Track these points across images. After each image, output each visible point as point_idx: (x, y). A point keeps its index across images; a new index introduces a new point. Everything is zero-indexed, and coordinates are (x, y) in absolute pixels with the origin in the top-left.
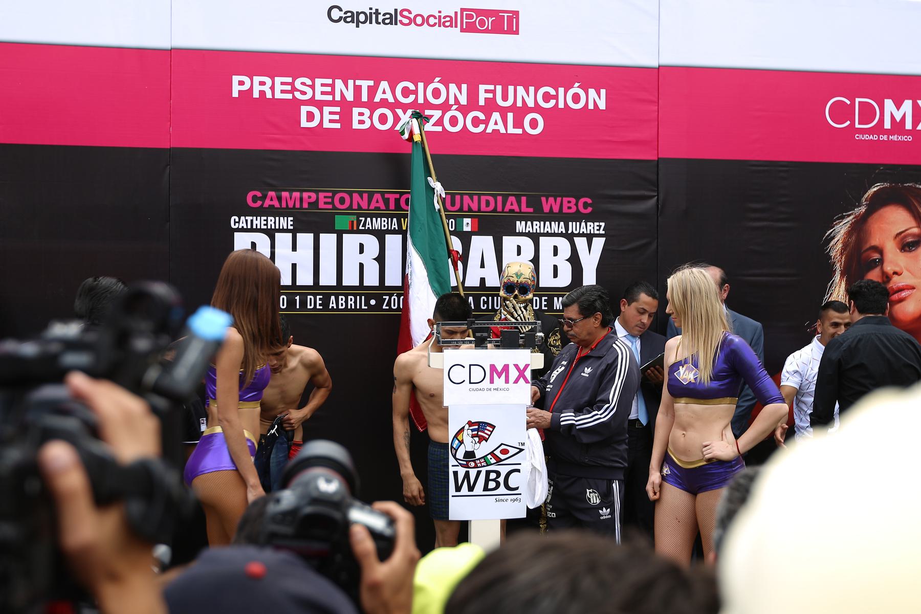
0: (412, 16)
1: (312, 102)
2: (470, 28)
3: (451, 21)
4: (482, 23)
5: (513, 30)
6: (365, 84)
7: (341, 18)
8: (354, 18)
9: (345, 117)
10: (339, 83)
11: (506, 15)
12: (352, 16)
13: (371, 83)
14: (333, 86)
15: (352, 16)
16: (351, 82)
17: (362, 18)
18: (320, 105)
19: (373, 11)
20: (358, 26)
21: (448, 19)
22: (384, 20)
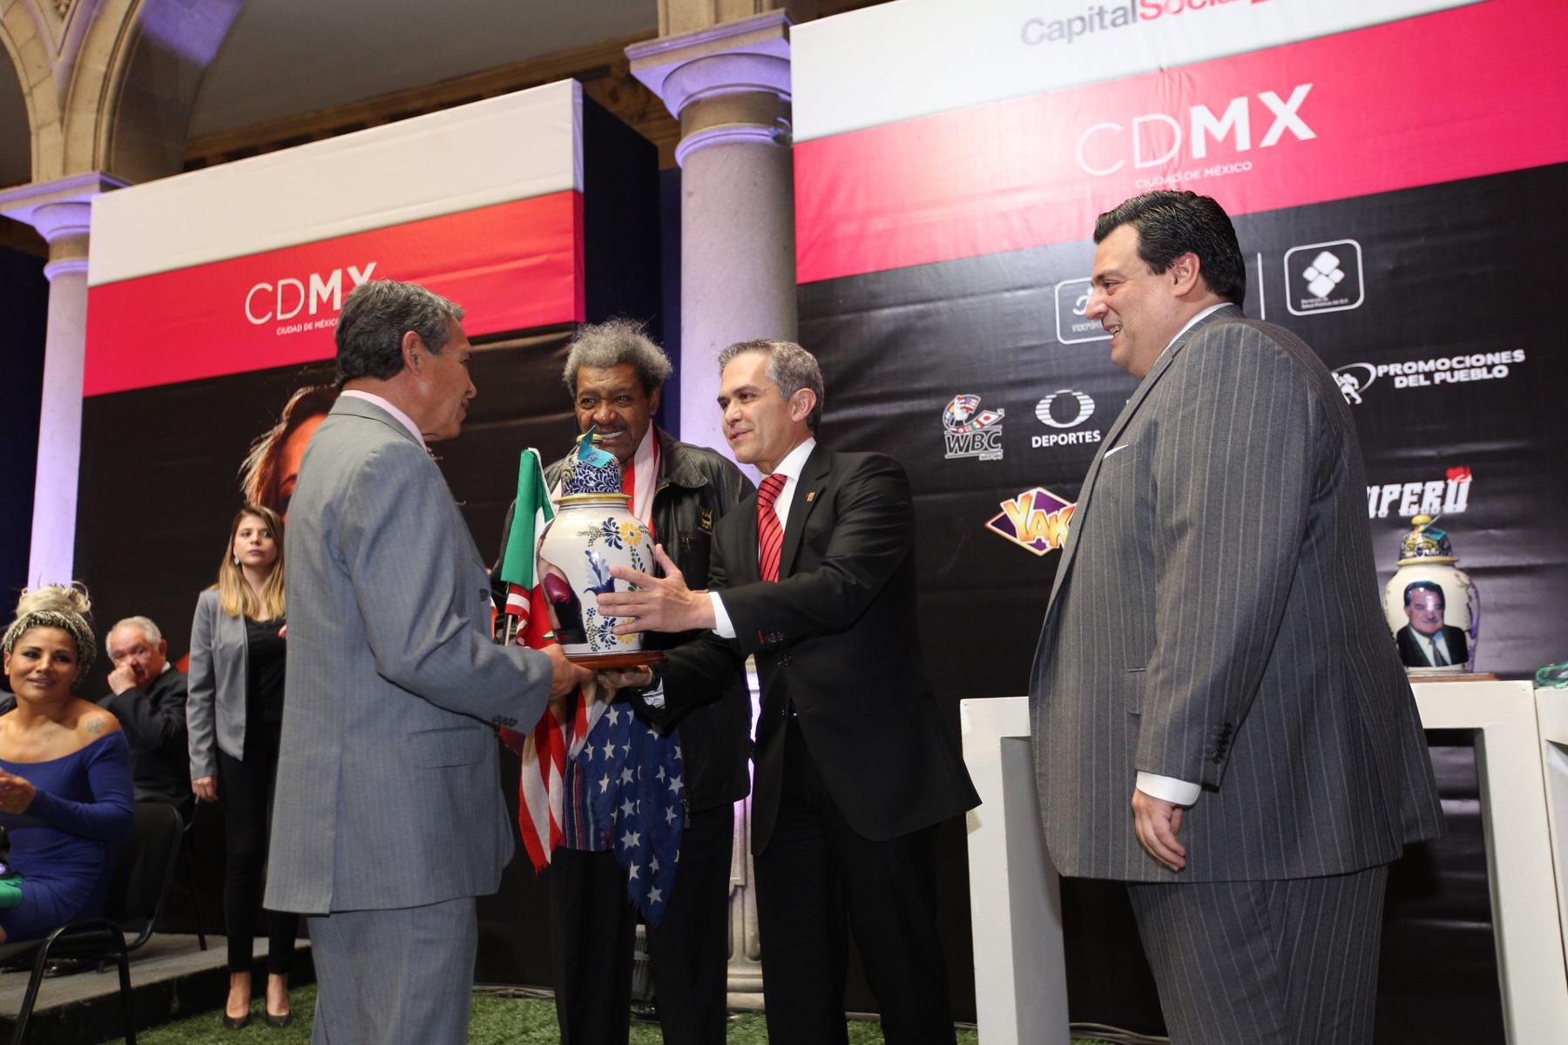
7: (1042, 37)
12: (1061, 29)
19: (1096, 10)
20: (1070, 41)
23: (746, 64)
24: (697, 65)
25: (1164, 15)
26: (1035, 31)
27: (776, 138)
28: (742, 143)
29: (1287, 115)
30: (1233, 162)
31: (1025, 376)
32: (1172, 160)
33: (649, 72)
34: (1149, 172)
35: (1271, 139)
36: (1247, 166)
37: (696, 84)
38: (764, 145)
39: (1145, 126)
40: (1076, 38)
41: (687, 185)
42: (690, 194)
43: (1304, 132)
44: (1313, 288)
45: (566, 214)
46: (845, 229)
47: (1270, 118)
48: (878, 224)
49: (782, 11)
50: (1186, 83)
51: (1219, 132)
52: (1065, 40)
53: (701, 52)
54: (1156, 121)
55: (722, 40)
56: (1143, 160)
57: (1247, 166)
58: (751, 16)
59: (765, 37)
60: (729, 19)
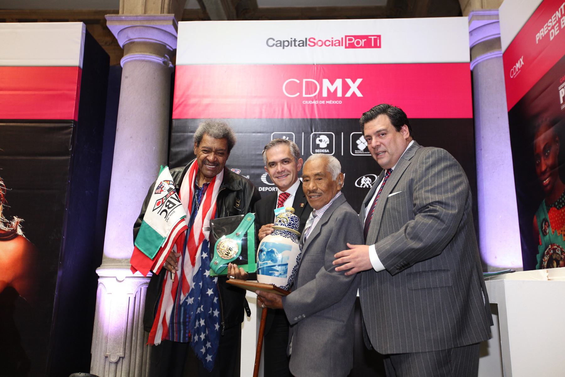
0: (315, 41)
2: (352, 46)
3: (339, 43)
4: (358, 43)
5: (377, 45)
7: (274, 45)
8: (282, 44)
11: (373, 38)
12: (281, 43)
15: (281, 43)
17: (286, 44)
19: (293, 39)
20: (283, 48)
21: (337, 42)
23: (156, 32)
24: (135, 28)
25: (316, 46)
26: (271, 42)
27: (164, 62)
28: (151, 62)
29: (354, 87)
30: (322, 100)
31: (258, 164)
32: (315, 96)
33: (114, 27)
34: (308, 99)
35: (349, 94)
36: (340, 102)
37: (134, 35)
38: (159, 64)
39: (306, 82)
41: (125, 74)
42: (126, 77)
43: (359, 94)
44: (359, 147)
45: (75, 77)
46: (192, 101)
47: (349, 87)
48: (206, 101)
49: (173, 15)
50: (322, 71)
51: (332, 89)
52: (282, 47)
53: (138, 24)
54: (311, 82)
55: (147, 20)
56: (306, 94)
57: (340, 102)
58: (159, 14)
59: (165, 23)
60: (151, 13)
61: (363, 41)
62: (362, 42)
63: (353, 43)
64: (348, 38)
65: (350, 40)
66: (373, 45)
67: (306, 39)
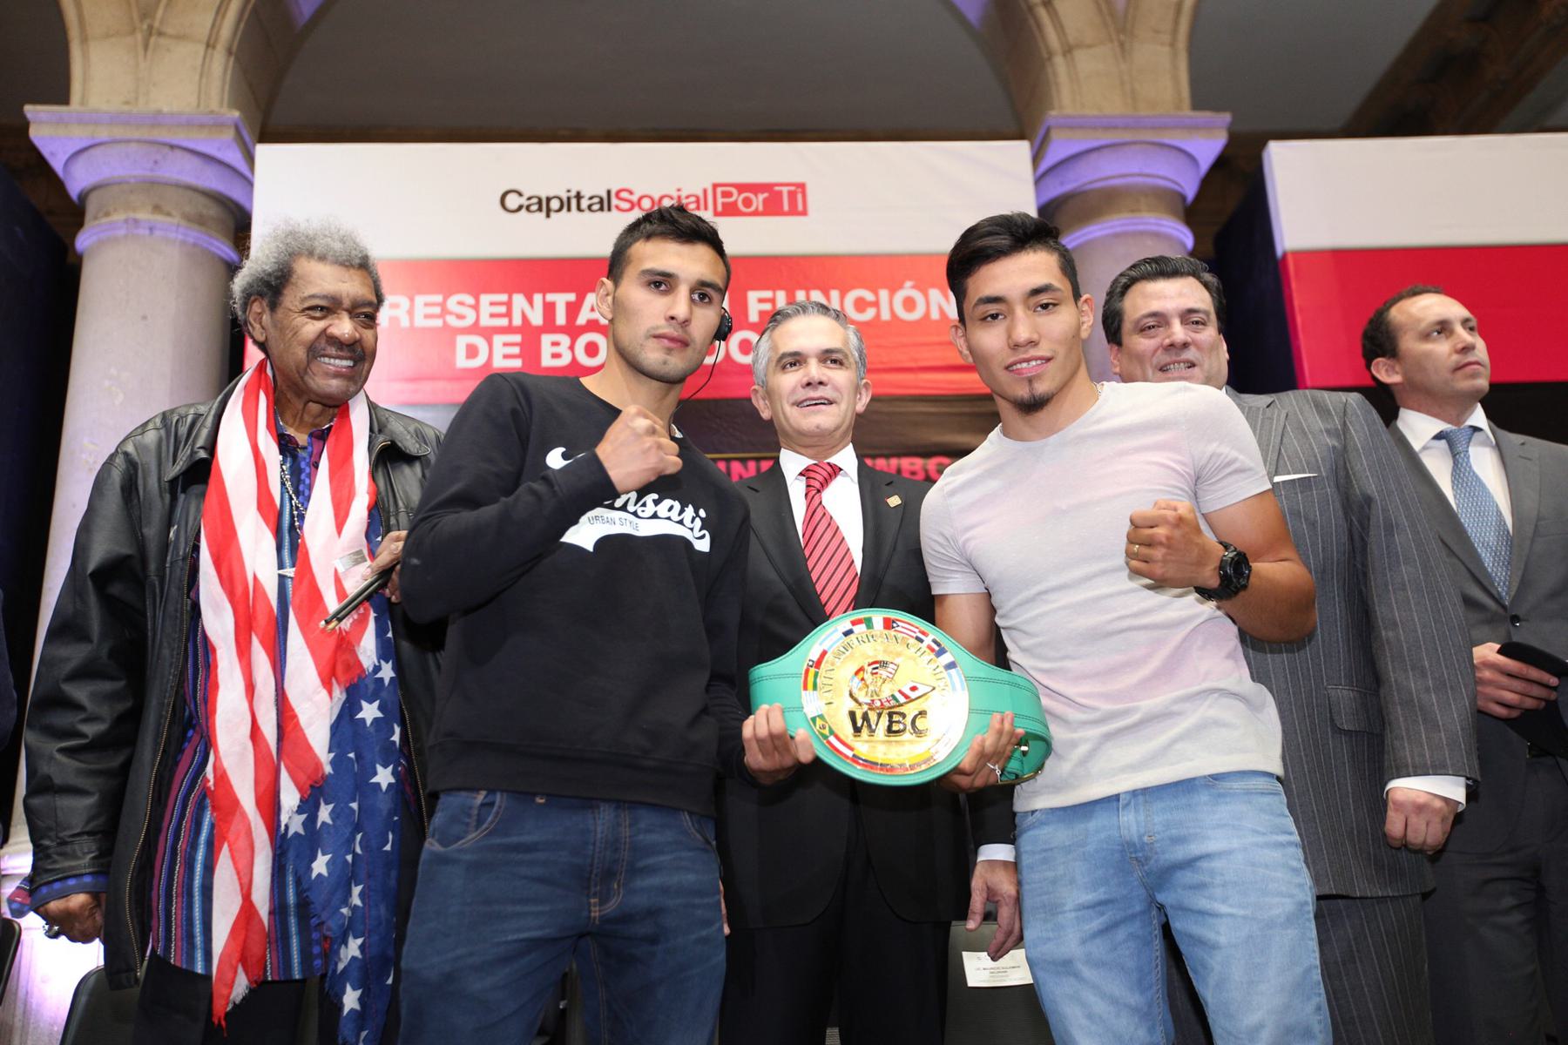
0: (635, 198)
1: (476, 329)
3: (698, 201)
4: (747, 202)
6: (561, 300)
7: (520, 208)
8: (543, 205)
9: (530, 348)
10: (519, 300)
12: (540, 202)
13: (572, 297)
14: (509, 304)
15: (540, 202)
16: (538, 298)
17: (555, 204)
18: (488, 334)
19: (573, 194)
20: (548, 216)
22: (590, 207)
40: (553, 215)
61: (762, 197)
62: (758, 201)
63: (735, 203)
64: (719, 190)
65: (727, 194)
66: (786, 207)
67: (609, 192)
